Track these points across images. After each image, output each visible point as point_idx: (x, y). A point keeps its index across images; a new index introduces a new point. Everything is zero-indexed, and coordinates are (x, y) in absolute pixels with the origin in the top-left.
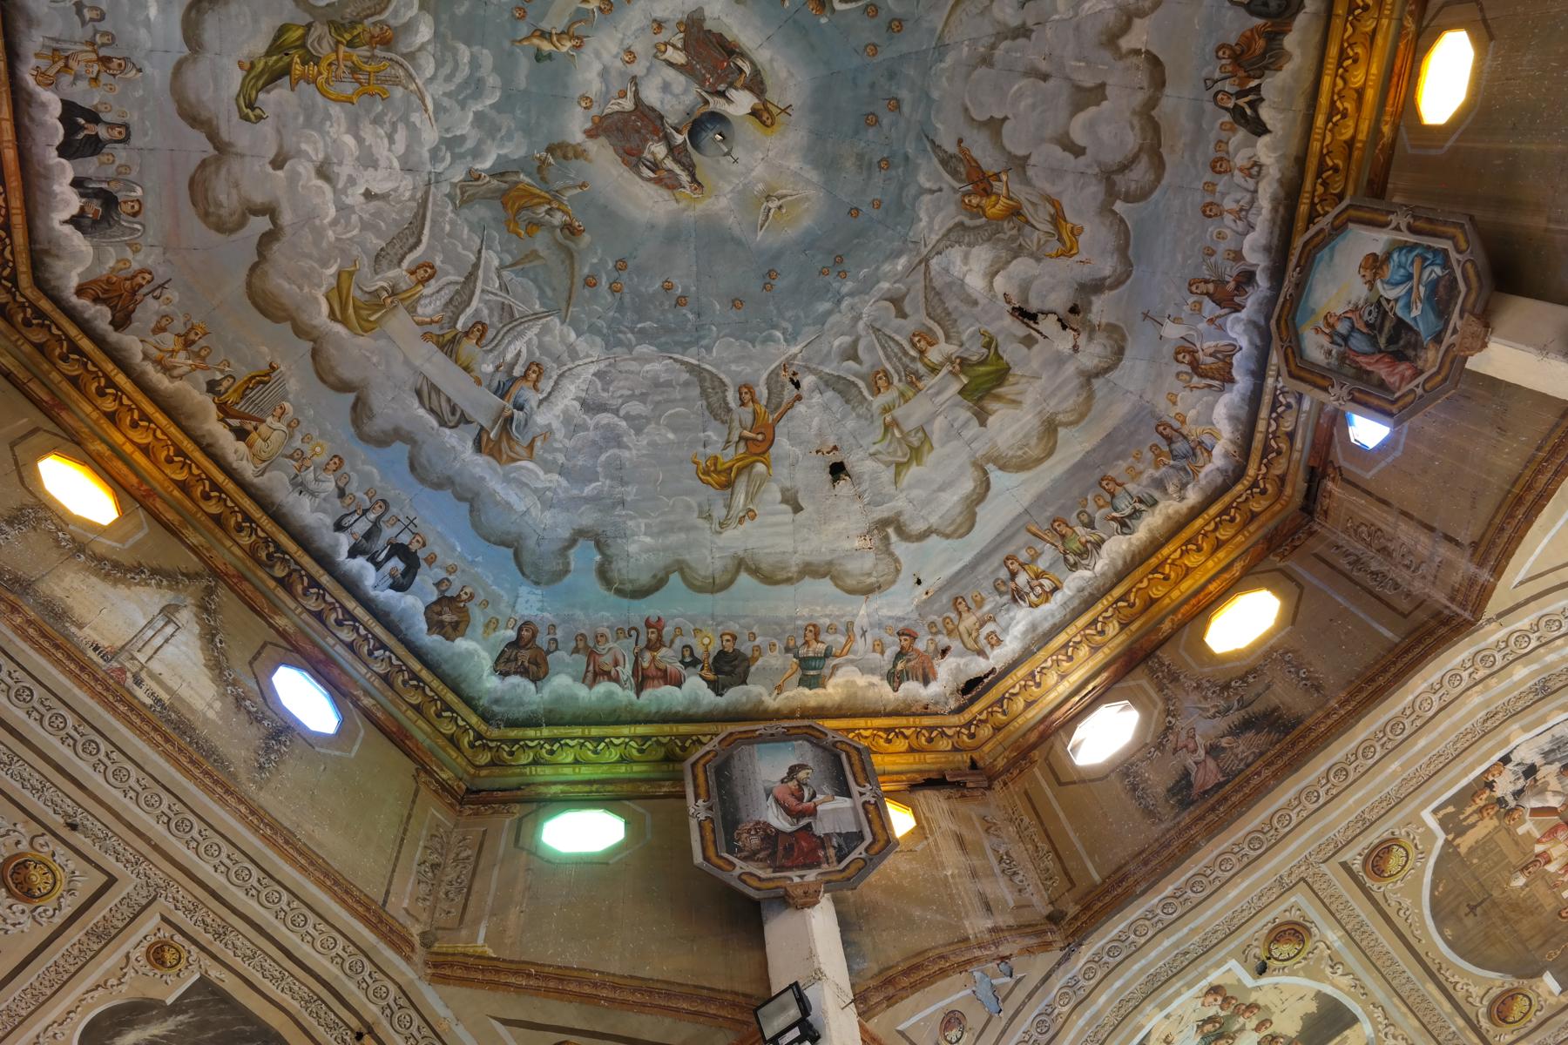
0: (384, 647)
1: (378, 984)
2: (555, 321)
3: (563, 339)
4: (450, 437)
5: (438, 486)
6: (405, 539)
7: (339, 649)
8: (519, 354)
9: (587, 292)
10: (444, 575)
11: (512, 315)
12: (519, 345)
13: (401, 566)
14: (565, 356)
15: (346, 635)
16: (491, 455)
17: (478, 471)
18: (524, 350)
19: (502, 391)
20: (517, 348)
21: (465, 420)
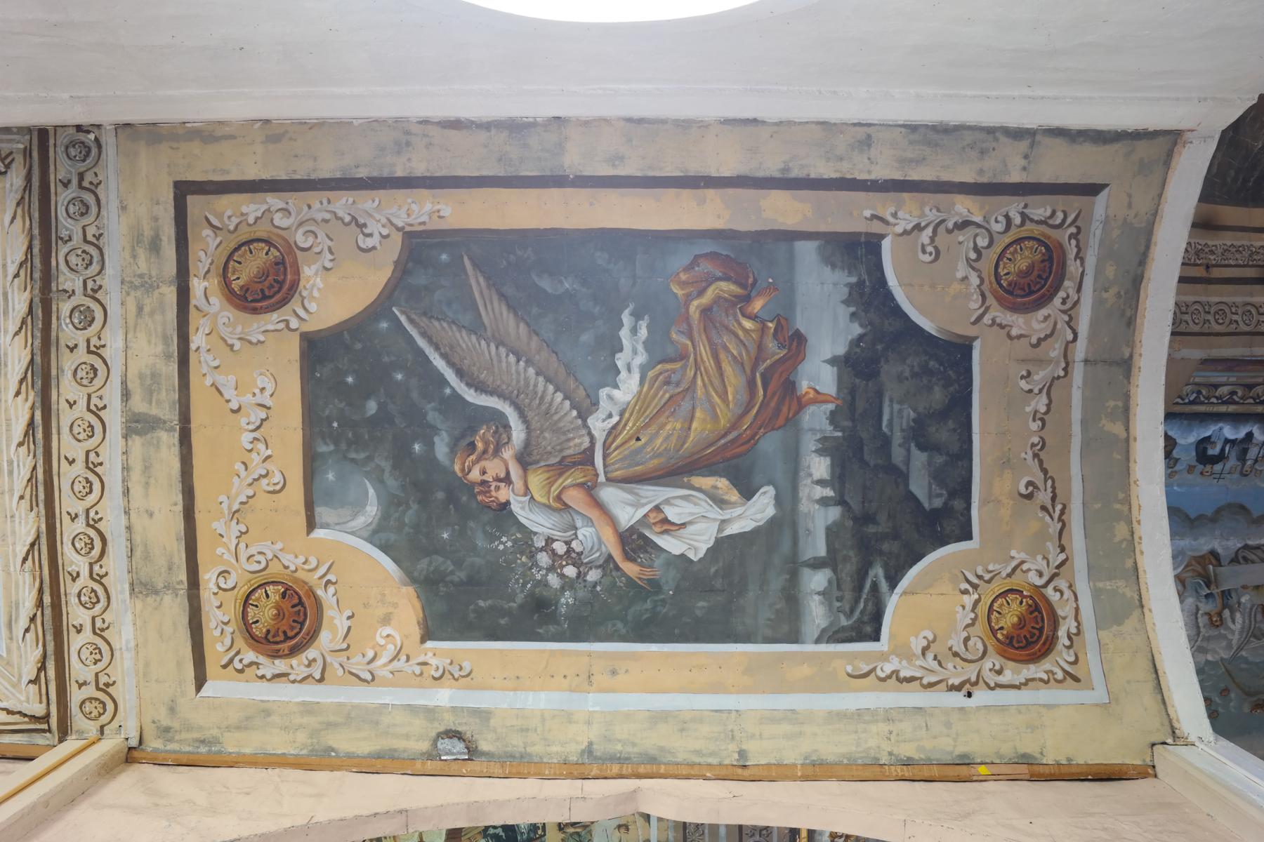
0: (1191, 403)
1: (1227, 321)
2: (1225, 655)
3: (1215, 652)
4: (1235, 544)
5: (1218, 511)
6: (1218, 467)
7: (1224, 379)
8: (1234, 622)
9: (1222, 686)
10: (1176, 468)
11: (1255, 637)
12: (1237, 627)
13: (1210, 452)
14: (1205, 644)
15: (1224, 390)
16: (1202, 557)
17: (1202, 540)
18: (1232, 626)
19: (1226, 594)
20: (1237, 624)
21: (1235, 560)
